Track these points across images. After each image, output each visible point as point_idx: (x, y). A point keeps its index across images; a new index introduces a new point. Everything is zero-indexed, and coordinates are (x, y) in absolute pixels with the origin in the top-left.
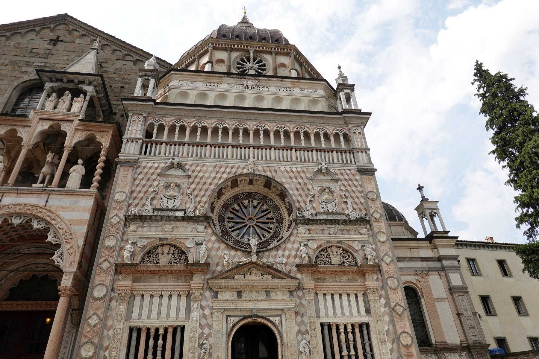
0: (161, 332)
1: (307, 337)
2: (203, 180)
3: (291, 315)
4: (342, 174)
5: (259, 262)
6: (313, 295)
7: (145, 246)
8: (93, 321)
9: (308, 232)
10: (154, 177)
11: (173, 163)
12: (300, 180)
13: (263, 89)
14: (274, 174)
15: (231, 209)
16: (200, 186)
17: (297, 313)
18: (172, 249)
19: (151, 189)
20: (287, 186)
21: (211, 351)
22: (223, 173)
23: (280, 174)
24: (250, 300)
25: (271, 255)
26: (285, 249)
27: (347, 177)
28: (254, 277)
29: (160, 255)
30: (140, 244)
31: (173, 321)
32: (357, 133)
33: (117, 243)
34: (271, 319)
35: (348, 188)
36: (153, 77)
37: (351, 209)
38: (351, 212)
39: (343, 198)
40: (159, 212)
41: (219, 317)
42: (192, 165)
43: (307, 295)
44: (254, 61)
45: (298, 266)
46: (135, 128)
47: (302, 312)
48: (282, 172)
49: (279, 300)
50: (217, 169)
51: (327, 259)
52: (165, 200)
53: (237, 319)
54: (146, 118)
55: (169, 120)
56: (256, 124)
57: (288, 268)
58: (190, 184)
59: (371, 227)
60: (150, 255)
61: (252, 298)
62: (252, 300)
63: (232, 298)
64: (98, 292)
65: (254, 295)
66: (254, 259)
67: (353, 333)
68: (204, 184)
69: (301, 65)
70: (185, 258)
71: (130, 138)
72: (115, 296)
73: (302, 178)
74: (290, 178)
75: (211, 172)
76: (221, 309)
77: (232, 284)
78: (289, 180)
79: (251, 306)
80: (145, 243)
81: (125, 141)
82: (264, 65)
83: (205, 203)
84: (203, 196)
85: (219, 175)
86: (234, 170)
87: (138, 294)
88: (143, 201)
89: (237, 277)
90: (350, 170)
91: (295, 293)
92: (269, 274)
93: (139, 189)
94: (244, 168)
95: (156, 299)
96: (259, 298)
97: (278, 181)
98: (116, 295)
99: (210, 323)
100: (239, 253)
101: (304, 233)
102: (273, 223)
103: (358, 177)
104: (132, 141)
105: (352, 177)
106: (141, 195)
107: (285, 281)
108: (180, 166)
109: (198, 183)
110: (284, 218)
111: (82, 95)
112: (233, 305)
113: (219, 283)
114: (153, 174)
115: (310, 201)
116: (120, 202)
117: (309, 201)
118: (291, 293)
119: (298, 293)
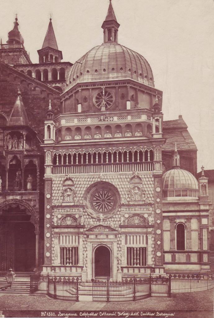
0: (71, 249)
1: (121, 252)
7: (61, 218)
8: (48, 245)
11: (67, 178)
13: (110, 119)
14: (112, 180)
20: (118, 187)
21: (87, 256)
23: (115, 180)
28: (102, 230)
29: (67, 221)
31: (75, 245)
32: (158, 150)
34: (107, 245)
36: (52, 124)
37: (146, 197)
38: (146, 199)
39: (143, 191)
43: (122, 237)
44: (105, 97)
46: (49, 159)
53: (97, 245)
57: (116, 226)
59: (154, 207)
64: (48, 235)
65: (102, 237)
66: (101, 223)
67: (140, 251)
68: (81, 188)
69: (135, 89)
79: (101, 240)
81: (45, 167)
82: (112, 97)
85: (87, 183)
89: (95, 230)
90: (150, 175)
91: (117, 236)
97: (113, 184)
100: (96, 220)
102: (113, 202)
108: (70, 179)
111: (21, 137)
117: (127, 194)
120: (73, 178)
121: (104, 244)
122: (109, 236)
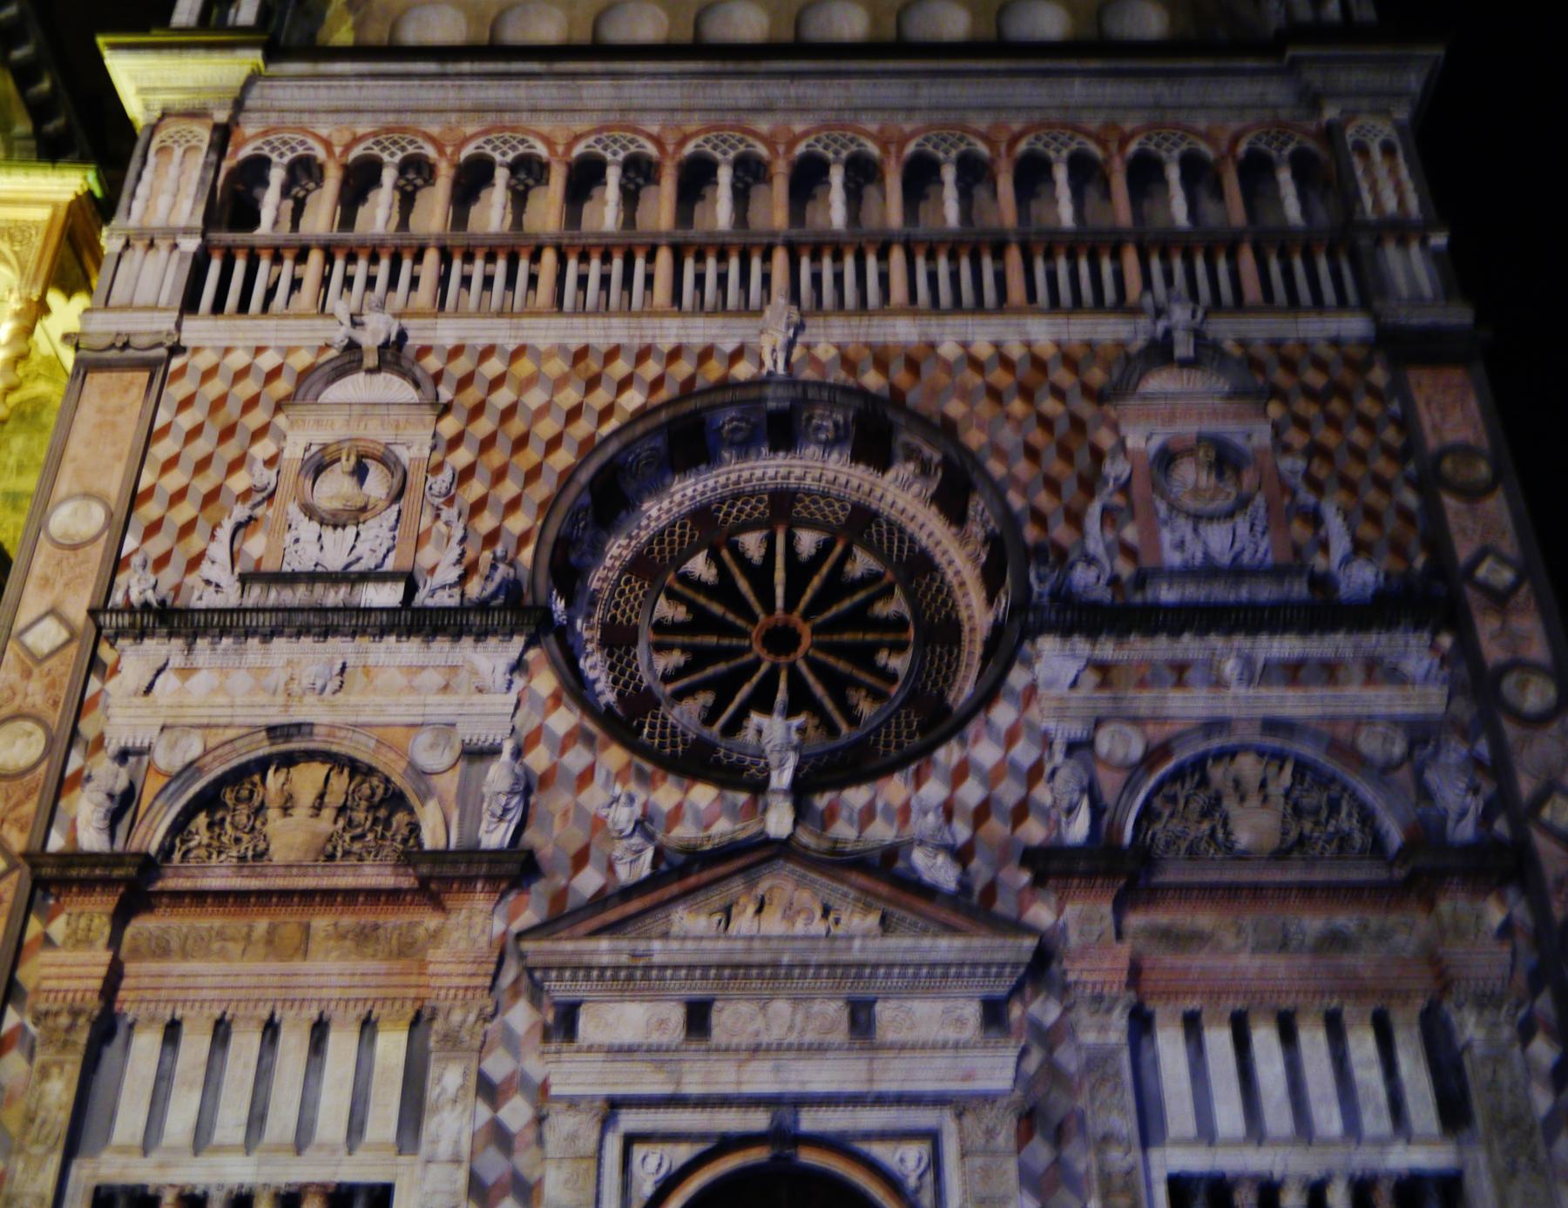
2: (517, 426)
3: (990, 1133)
4: (1289, 365)
5: (806, 838)
6: (1118, 1022)
9: (1090, 678)
10: (256, 418)
12: (1050, 406)
14: (900, 375)
15: (670, 577)
16: (497, 457)
17: (1030, 1120)
18: (340, 783)
19: (239, 482)
20: (974, 439)
22: (624, 384)
24: (756, 1050)
25: (880, 804)
26: (959, 774)
27: (1315, 379)
29: (273, 813)
30: (168, 758)
33: (48, 751)
34: (879, 1151)
35: (1328, 437)
37: (1340, 544)
38: (1346, 561)
40: (273, 594)
41: (580, 1143)
42: (456, 352)
45: (1032, 857)
47: (1057, 1115)
48: (948, 367)
49: (924, 1047)
50: (594, 365)
51: (1206, 826)
52: (308, 529)
53: (682, 1153)
54: (223, 136)
55: (347, 137)
56: (806, 134)
58: (442, 446)
60: (218, 816)
61: (765, 1039)
62: (768, 1049)
63: (656, 1038)
66: (779, 821)
68: (521, 443)
70: (405, 831)
71: (140, 232)
72: (21, 1028)
73: (1059, 393)
74: (995, 394)
75: (559, 383)
76: (593, 1098)
77: (657, 959)
78: (984, 407)
79: (761, 1079)
80: (195, 750)
83: (523, 540)
84: (513, 505)
85: (601, 398)
86: (684, 368)
87: (152, 1019)
88: (196, 542)
91: (1016, 1011)
92: (868, 909)
93: (175, 480)
94: (737, 355)
95: (245, 1044)
96: (809, 1037)
98: (28, 1021)
99: (531, 1175)
101: (1074, 684)
103: (1379, 376)
104: (151, 245)
105: (1343, 374)
106: (186, 511)
107: (958, 942)
109: (487, 444)
110: (963, 614)
112: (661, 1077)
113: (581, 953)
114: (251, 404)
115: (1107, 513)
116: (75, 547)
117: (1095, 509)
118: (994, 1014)
119: (1035, 1008)
120: (424, 351)
121: (819, 1141)
122: (885, 1012)
